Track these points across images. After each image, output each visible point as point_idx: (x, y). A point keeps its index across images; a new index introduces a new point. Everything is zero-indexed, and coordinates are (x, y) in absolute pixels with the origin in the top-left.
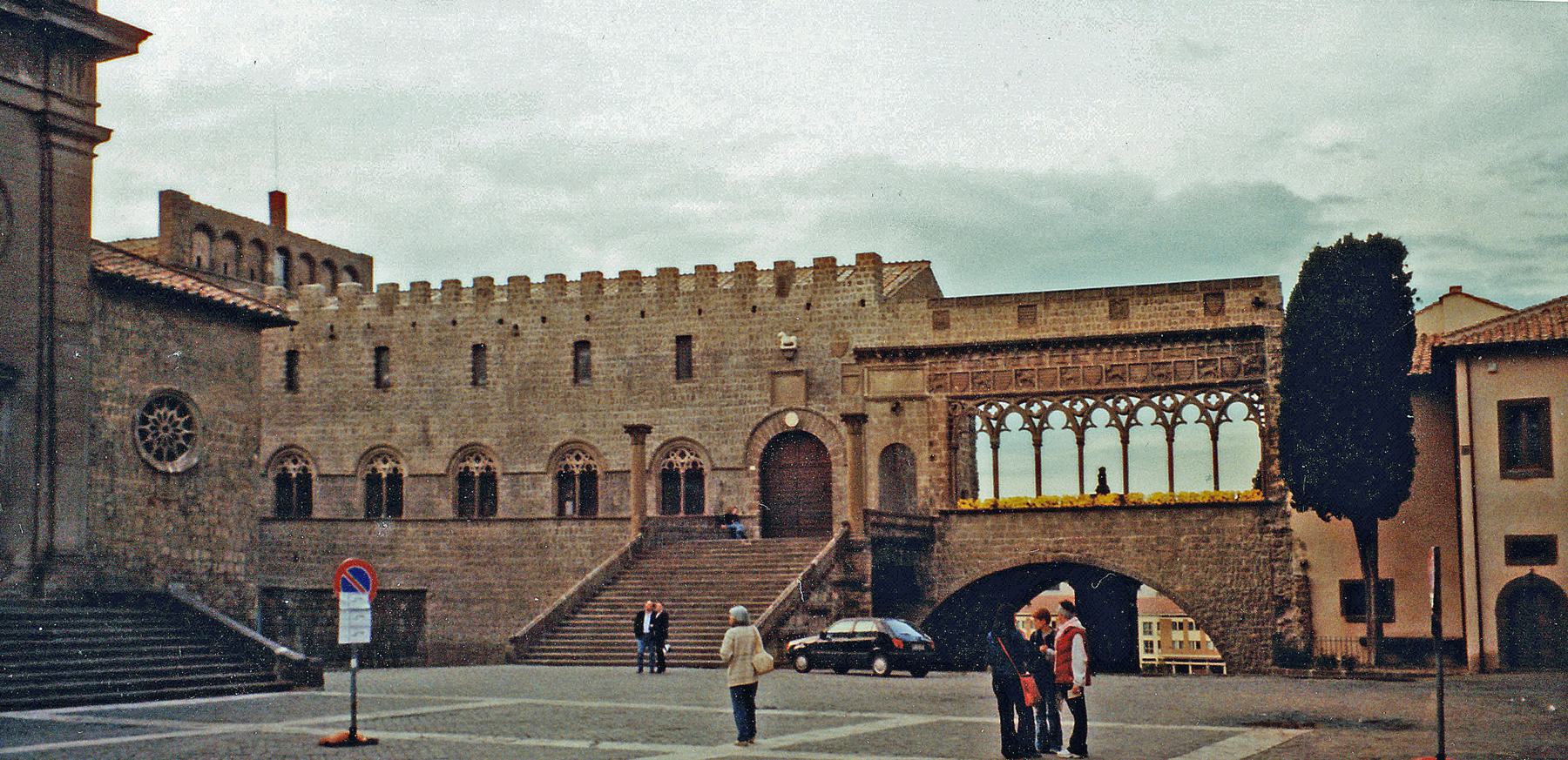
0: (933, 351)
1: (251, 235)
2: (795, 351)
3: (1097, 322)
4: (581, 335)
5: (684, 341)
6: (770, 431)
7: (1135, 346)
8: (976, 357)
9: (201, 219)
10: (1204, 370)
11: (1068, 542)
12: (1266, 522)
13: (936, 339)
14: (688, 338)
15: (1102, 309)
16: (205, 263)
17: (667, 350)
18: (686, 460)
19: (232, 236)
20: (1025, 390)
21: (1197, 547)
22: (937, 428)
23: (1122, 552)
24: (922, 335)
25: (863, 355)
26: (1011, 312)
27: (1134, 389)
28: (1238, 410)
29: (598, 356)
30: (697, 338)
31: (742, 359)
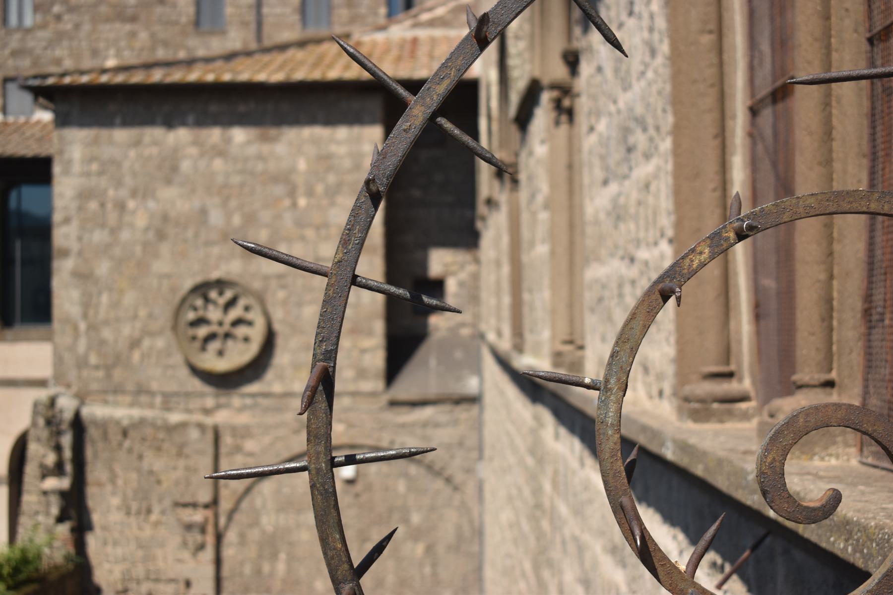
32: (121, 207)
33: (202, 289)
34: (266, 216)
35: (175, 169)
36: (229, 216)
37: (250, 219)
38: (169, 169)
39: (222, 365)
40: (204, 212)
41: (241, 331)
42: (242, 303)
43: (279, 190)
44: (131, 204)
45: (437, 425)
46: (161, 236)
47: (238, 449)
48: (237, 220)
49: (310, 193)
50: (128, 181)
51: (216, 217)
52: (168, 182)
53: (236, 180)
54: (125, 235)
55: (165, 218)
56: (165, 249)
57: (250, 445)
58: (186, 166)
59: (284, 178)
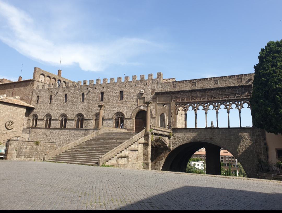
0: (173, 93)
1: (53, 77)
2: (143, 93)
3: (211, 85)
4: (102, 91)
5: (122, 92)
6: (138, 110)
7: (220, 90)
8: (182, 94)
9: (42, 73)
10: (237, 96)
11: (205, 138)
12: (254, 133)
13: (172, 90)
14: (123, 91)
15: (212, 82)
16: (43, 81)
17: (118, 94)
18: (120, 116)
19: (48, 76)
20: (193, 101)
21: (236, 139)
22: (173, 110)
23: (217, 141)
24: (170, 89)
25: (157, 94)
26: (190, 84)
27: (220, 100)
28: (246, 105)
29: (105, 95)
30: (124, 91)
31: (132, 95)
32: (2, 113)
33: (9, 121)
34: (15, 116)
35: (8, 110)
36: (12, 115)
37: (14, 116)
38: (7, 110)
39: (10, 128)
40: (10, 115)
41: (11, 125)
42: (12, 123)
43: (17, 114)
44: (3, 113)
45: (26, 135)
46: (5, 116)
47: (9, 136)
48: (13, 116)
49: (19, 114)
50: (3, 111)
51: (11, 115)
52: (7, 111)
53: (13, 112)
54: (2, 115)
55: (6, 114)
56: (6, 117)
57: (10, 136)
58: (9, 110)
59: (17, 113)
